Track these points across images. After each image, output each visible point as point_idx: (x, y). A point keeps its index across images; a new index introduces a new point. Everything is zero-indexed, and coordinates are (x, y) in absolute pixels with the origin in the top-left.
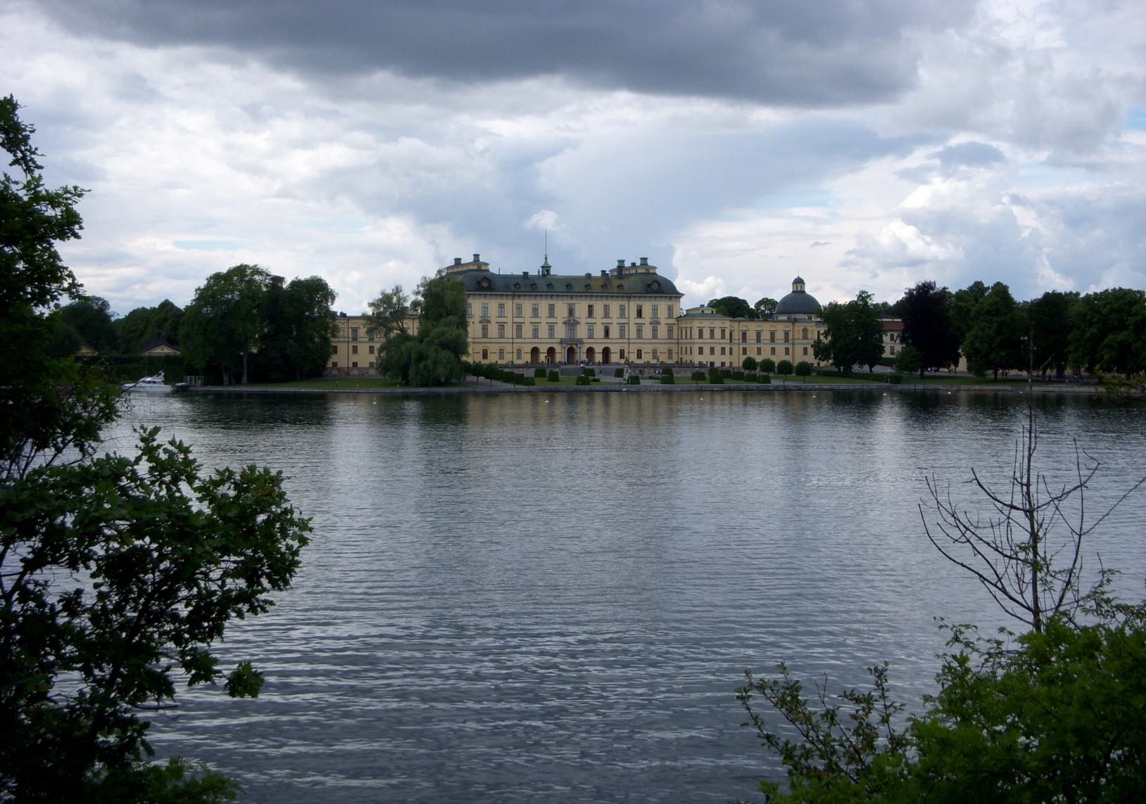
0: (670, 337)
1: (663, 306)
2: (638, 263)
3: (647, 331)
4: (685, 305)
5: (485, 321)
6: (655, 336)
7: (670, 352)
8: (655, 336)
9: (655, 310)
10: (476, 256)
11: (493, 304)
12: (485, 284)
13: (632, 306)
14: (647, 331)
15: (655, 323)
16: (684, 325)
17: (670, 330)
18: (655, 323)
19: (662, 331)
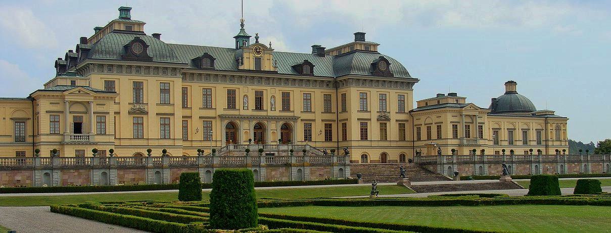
0: (402, 138)
1: (393, 95)
2: (352, 39)
3: (374, 131)
4: (419, 94)
5: (138, 113)
6: (384, 137)
7: (402, 157)
8: (384, 137)
9: (383, 99)
10: (125, 11)
11: (152, 85)
12: (137, 50)
13: (354, 93)
14: (374, 131)
15: (384, 120)
16: (422, 121)
17: (402, 127)
18: (384, 120)
19: (393, 130)
